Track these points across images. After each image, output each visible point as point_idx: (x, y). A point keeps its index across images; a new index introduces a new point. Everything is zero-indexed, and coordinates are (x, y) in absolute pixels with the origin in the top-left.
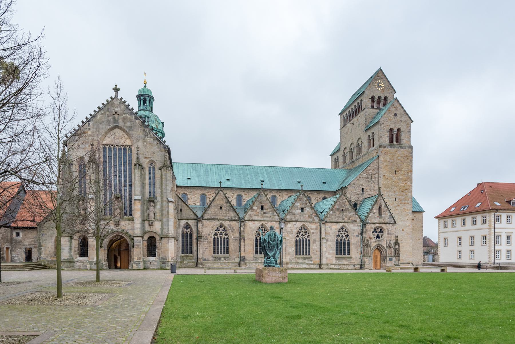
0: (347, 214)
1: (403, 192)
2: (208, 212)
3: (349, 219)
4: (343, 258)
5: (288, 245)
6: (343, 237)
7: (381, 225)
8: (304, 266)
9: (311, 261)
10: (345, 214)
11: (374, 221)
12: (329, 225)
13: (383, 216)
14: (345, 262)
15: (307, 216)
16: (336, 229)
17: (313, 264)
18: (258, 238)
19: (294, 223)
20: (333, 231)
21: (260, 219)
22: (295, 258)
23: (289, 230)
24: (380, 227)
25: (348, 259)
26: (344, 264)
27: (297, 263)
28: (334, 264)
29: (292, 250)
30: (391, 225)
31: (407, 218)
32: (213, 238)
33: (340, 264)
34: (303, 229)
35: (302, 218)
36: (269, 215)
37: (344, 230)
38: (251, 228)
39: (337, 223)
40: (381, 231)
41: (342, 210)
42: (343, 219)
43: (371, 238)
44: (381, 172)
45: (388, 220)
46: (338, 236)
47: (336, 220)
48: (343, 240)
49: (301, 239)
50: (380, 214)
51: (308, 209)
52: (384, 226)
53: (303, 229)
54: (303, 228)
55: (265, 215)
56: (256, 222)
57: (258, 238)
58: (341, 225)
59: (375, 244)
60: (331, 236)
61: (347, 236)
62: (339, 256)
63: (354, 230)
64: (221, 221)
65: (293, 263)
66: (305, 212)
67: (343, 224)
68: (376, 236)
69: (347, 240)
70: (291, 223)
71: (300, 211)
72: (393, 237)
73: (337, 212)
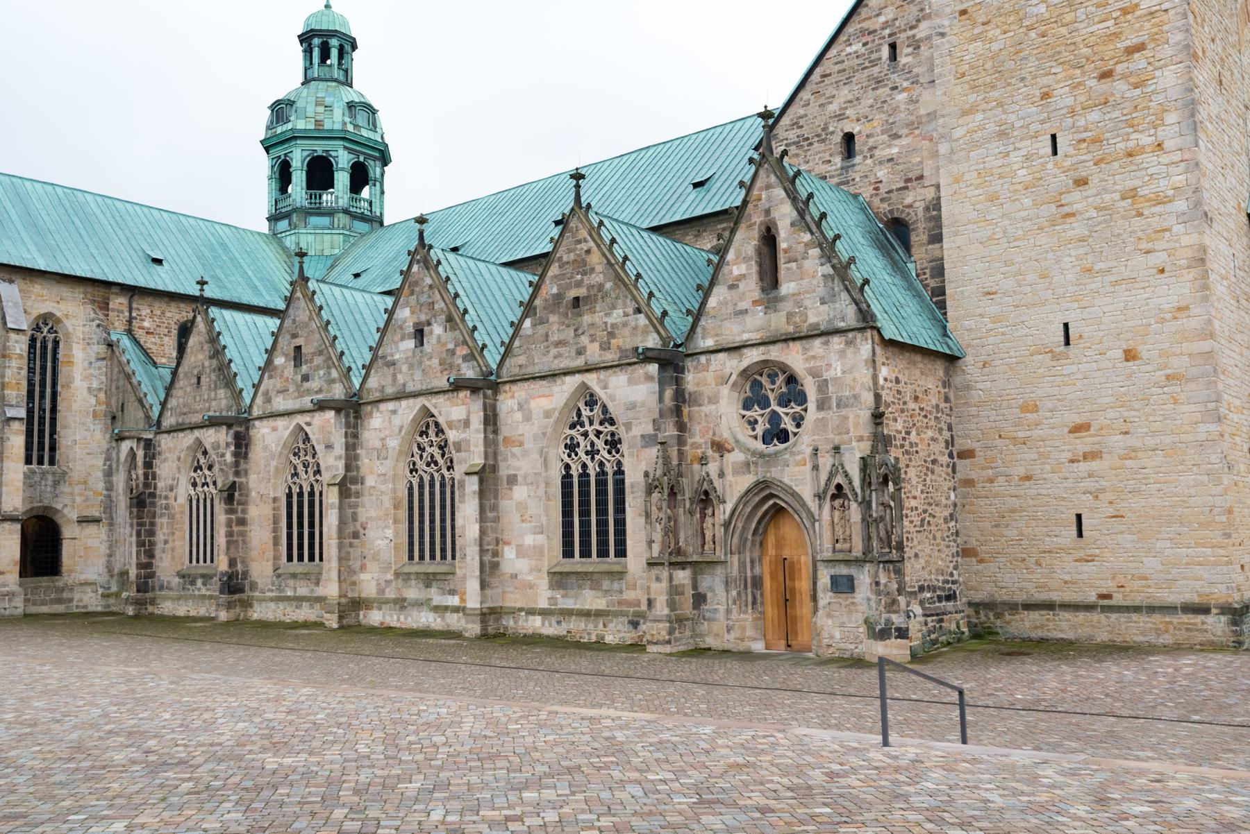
0: (598, 318)
2: (173, 403)
3: (605, 347)
4: (584, 576)
5: (373, 514)
6: (592, 453)
7: (775, 353)
8: (425, 619)
9: (452, 592)
10: (587, 319)
11: (735, 332)
12: (520, 391)
13: (786, 288)
14: (591, 600)
15: (436, 361)
16: (547, 414)
17: (456, 610)
18: (296, 490)
19: (391, 406)
20: (538, 423)
22: (397, 575)
23: (378, 444)
24: (784, 368)
25: (606, 584)
26: (586, 614)
27: (401, 604)
28: (544, 613)
29: (384, 534)
30: (837, 341)
33: (569, 613)
34: (432, 432)
35: (418, 375)
36: (314, 384)
37: (597, 409)
38: (266, 448)
39: (553, 376)
40: (794, 393)
41: (577, 299)
42: (580, 352)
43: (720, 448)
45: (817, 315)
46: (572, 447)
47: (544, 363)
49: (427, 478)
50: (770, 277)
51: (437, 329)
52: (795, 358)
53: (432, 432)
54: (427, 425)
55: (306, 385)
56: (281, 423)
57: (296, 490)
58: (572, 382)
59: (747, 481)
60: (526, 453)
61: (614, 444)
62: (577, 563)
63: (632, 406)
64: (197, 433)
65: (387, 602)
66: (427, 347)
67: (578, 378)
68: (760, 429)
69: (609, 469)
70: (383, 406)
71: (411, 343)
72: (860, 418)
73: (553, 318)
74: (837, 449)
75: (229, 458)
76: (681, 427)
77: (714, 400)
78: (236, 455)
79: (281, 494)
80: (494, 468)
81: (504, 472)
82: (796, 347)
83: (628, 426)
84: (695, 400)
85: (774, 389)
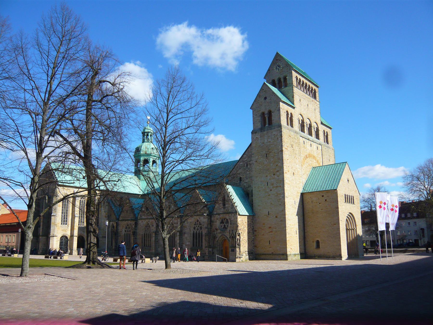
1: (274, 174)
6: (198, 229)
13: (226, 206)
21: (145, 217)
31: (280, 203)
32: (123, 234)
43: (217, 229)
44: (254, 159)
48: (198, 232)
56: (143, 221)
63: (204, 222)
68: (223, 227)
74: (232, 230)
75: (134, 227)
76: (211, 226)
77: (216, 222)
78: (135, 226)
79: (143, 234)
80: (182, 231)
81: (183, 232)
82: (227, 215)
83: (203, 225)
84: (213, 222)
85: (225, 221)
